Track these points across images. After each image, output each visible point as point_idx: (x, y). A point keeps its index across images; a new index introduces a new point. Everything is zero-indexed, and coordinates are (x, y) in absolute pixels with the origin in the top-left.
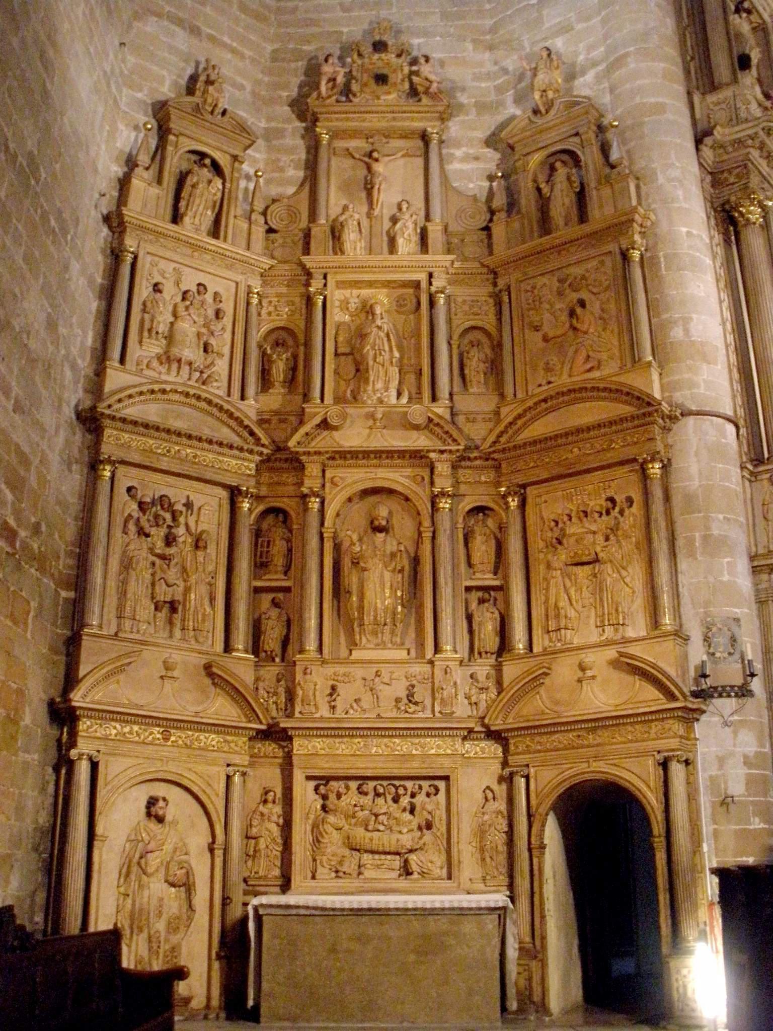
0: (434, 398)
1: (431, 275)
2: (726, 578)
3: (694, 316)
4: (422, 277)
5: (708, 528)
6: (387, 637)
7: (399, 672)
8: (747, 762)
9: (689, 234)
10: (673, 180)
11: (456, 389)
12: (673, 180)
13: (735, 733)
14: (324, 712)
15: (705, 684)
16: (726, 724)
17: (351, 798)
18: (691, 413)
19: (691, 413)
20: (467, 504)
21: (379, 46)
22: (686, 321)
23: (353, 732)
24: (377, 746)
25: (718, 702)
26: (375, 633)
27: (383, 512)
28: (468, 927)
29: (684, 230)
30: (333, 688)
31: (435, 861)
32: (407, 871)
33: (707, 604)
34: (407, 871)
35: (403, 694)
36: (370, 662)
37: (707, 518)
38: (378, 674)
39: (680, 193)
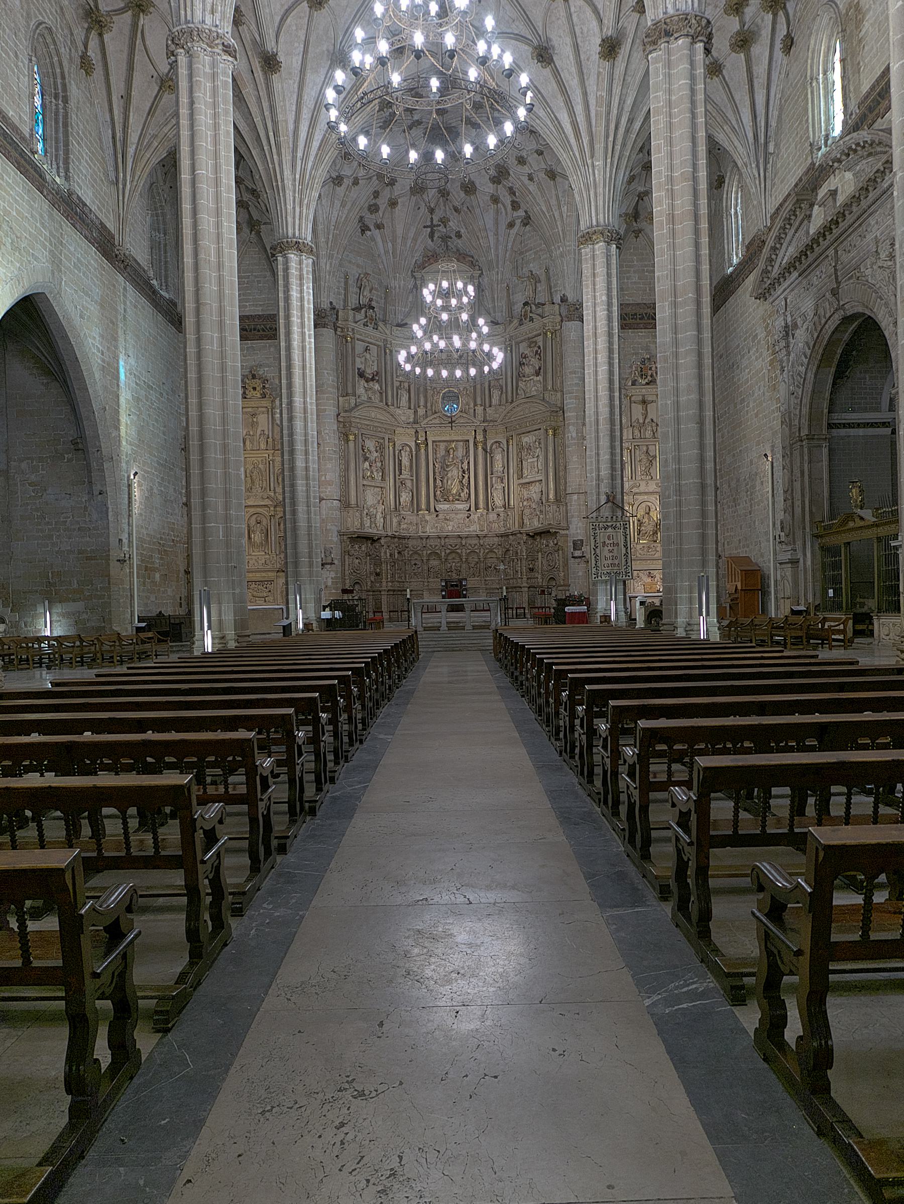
4: (267, 455)
7: (263, 557)
8: (332, 578)
17: (253, 586)
20: (279, 516)
21: (254, 377)
23: (252, 572)
24: (258, 575)
28: (276, 612)
31: (271, 598)
32: (265, 601)
34: (265, 601)
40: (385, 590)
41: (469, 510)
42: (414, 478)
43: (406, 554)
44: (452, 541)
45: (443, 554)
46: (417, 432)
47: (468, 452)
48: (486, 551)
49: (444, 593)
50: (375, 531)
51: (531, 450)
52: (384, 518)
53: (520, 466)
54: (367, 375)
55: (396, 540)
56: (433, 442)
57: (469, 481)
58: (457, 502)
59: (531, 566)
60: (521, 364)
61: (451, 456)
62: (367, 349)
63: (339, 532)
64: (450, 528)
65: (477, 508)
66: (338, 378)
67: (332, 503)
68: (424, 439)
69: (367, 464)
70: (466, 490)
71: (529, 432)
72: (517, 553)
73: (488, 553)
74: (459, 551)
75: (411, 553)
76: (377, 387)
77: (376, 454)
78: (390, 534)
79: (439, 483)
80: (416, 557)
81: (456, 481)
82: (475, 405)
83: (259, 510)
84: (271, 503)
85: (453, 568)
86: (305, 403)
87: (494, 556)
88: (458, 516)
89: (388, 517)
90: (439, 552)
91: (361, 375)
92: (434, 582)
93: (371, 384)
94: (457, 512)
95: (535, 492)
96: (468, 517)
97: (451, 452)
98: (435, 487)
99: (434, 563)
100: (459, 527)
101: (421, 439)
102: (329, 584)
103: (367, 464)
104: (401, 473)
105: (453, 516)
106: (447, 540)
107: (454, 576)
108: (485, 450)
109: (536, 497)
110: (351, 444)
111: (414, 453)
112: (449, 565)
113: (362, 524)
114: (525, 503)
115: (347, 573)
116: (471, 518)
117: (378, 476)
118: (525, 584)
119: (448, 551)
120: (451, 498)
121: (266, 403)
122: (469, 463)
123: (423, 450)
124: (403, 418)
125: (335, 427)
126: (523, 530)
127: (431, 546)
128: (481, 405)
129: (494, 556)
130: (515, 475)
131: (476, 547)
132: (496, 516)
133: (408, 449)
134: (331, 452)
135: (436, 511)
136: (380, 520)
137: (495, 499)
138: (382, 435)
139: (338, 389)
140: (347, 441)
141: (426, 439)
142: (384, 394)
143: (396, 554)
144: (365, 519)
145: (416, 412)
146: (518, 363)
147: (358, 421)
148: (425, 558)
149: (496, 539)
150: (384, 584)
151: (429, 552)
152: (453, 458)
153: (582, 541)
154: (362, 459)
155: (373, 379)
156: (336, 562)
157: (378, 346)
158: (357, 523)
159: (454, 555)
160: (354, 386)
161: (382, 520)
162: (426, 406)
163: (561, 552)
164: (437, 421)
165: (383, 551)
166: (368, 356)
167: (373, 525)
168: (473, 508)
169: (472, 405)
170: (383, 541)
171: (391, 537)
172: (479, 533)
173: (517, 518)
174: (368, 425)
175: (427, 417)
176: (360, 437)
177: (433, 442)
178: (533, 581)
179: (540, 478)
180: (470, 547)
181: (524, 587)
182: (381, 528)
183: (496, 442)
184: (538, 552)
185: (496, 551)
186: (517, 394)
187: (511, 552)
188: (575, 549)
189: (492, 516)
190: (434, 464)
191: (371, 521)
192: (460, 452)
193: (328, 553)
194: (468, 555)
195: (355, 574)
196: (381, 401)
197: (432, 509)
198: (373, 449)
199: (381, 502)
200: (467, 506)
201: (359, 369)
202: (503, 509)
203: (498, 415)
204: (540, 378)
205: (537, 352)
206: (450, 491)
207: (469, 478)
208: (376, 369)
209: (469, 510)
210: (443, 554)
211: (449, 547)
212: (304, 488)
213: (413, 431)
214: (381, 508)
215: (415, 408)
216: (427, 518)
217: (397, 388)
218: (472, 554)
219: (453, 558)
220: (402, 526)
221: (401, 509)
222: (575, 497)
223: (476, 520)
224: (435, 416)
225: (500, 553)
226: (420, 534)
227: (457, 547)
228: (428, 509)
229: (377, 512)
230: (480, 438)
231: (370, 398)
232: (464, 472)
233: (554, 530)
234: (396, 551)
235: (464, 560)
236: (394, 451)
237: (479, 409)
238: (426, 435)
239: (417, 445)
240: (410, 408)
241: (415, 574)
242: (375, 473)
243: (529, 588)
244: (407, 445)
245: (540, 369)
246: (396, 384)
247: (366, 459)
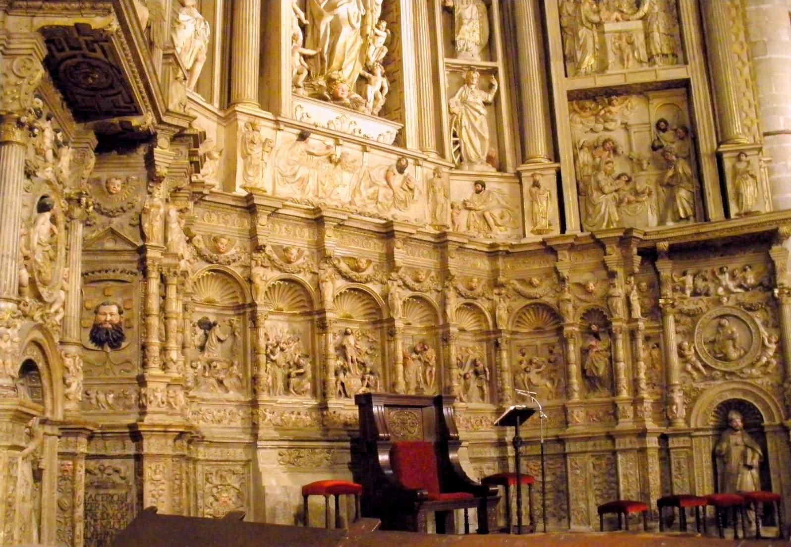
64: (343, 195)
70: (379, 81)
74: (375, 289)
85: (351, 352)
90: (305, 278)
96: (401, 170)
100: (375, 199)
179: (678, 73)
185: (484, 305)
202: (492, 171)
219: (348, 319)
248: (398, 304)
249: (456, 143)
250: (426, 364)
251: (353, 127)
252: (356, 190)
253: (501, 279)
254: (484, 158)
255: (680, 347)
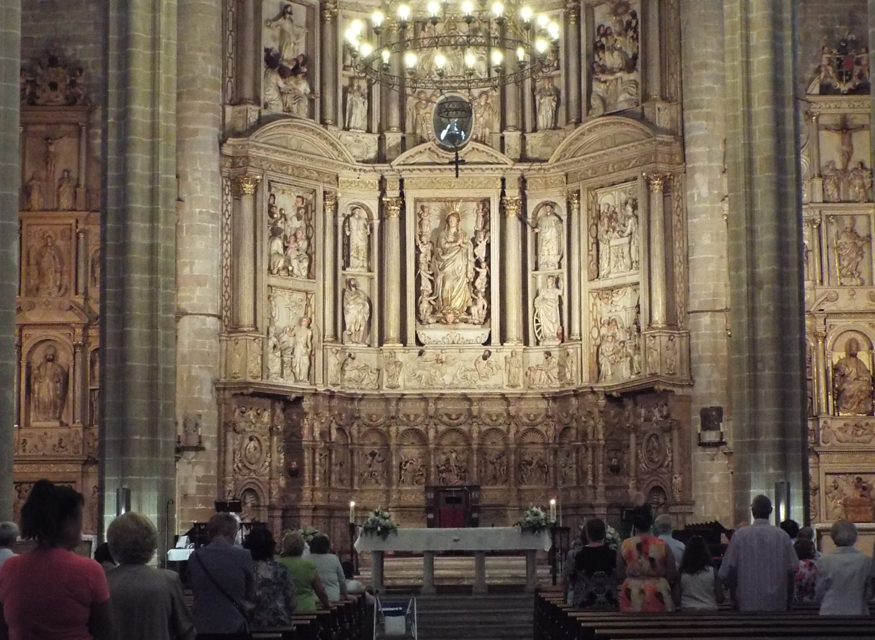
0: (77, 293)
1: (77, 222)
2: (196, 396)
3: (196, 261)
4: (73, 221)
5: (190, 372)
6: (51, 415)
8: (198, 480)
9: (201, 212)
10: (194, 180)
11: (89, 286)
12: (194, 180)
13: (193, 467)
14: (21, 453)
15: (635, 287)
16: (190, 463)
18: (187, 314)
19: (186, 314)
22: (192, 264)
23: (32, 462)
25: (186, 453)
26: (44, 413)
27: (51, 351)
29: (198, 210)
30: (25, 441)
33: (186, 407)
35: (56, 442)
36: (42, 428)
37: (190, 367)
38: (46, 434)
39: (199, 188)
40: (307, 507)
41: (488, 342)
42: (375, 274)
43: (355, 432)
44: (451, 407)
45: (432, 434)
46: (382, 182)
47: (487, 221)
48: (522, 429)
49: (431, 516)
50: (290, 382)
51: (616, 220)
52: (311, 356)
53: (594, 252)
54: (285, 64)
55: (335, 402)
56: (417, 201)
57: (489, 283)
58: (463, 325)
59: (614, 461)
60: (599, 48)
61: (453, 230)
62: (285, 12)
63: (216, 382)
64: (448, 379)
65: (503, 339)
66: (225, 67)
67: (204, 324)
68: (397, 193)
69: (277, 245)
70: (482, 302)
71: (613, 184)
72: (585, 435)
73: (525, 434)
74: (464, 428)
75: (364, 429)
76: (303, 87)
77: (295, 224)
78: (321, 389)
79: (426, 286)
80: (375, 438)
81: (463, 282)
82: (503, 127)
83: (52, 333)
84: (76, 319)
85: (453, 463)
86: (154, 115)
87: (538, 438)
88: (463, 355)
89: (319, 355)
90: (422, 428)
91: (273, 61)
92: (412, 492)
93: (292, 81)
94: (460, 346)
95: (625, 308)
97: (453, 220)
98: (418, 293)
99: (411, 452)
100: (465, 377)
101: (392, 193)
102: (192, 491)
103: (277, 245)
104: (347, 264)
105: (452, 353)
106: (440, 405)
107: (454, 480)
108: (522, 218)
109: (626, 318)
110: (247, 204)
111: (376, 223)
112: (443, 457)
113: (264, 367)
114: (604, 331)
115: (230, 468)
116: (491, 359)
117: (300, 267)
118: (601, 500)
119: (442, 428)
120: (450, 317)
121: (75, 116)
122: (488, 246)
123: (394, 218)
124: (356, 152)
125: (215, 167)
126: (599, 387)
127: (407, 416)
128: (516, 129)
129: (538, 438)
130: (584, 273)
131: (501, 420)
132: (542, 356)
133: (364, 214)
134: (205, 217)
135: (418, 343)
136: (301, 360)
137: (541, 320)
138: (311, 184)
139: (224, 89)
140: (238, 193)
141: (402, 195)
142: (318, 102)
143: (334, 433)
144: (271, 356)
145: (381, 140)
146: (591, 47)
147: (262, 153)
148: (393, 442)
149: (543, 404)
150: (307, 494)
151: (402, 429)
152: (456, 235)
153: (719, 410)
154: (267, 233)
155: (295, 72)
156: (207, 445)
157: (310, 7)
158: (254, 366)
159: (454, 436)
160: (256, 85)
161: (306, 360)
162: (402, 128)
163: (675, 433)
164: (425, 158)
165: (306, 423)
166: (287, 25)
167: (287, 371)
168: (496, 339)
169: (497, 126)
170: (306, 404)
171: (324, 395)
172: (507, 390)
173: (586, 362)
174: (283, 165)
175: (404, 150)
176: (266, 188)
177: (417, 201)
178: (618, 493)
180: (488, 420)
181: (599, 506)
182: (303, 376)
183: (546, 204)
184: (629, 434)
186: (589, 107)
187: (573, 431)
188: (706, 427)
189: (536, 356)
190: (417, 247)
191: (283, 362)
192: (472, 223)
193: (191, 426)
194: (483, 436)
195: (245, 471)
196: (311, 116)
197: (411, 339)
198: (290, 212)
199: (305, 322)
200: (482, 334)
201: (268, 51)
202: (558, 342)
203: (549, 150)
204: (634, 76)
205: (629, 23)
206: (447, 302)
207: (488, 276)
208: (302, 50)
209: (488, 342)
210: (432, 434)
211: (445, 419)
212: (146, 290)
213: (374, 178)
214: (304, 334)
215: (381, 131)
216: (401, 357)
217: (345, 91)
218: (493, 435)
219: (454, 444)
220: (348, 374)
221: (346, 338)
222: (706, 319)
223: (502, 362)
224: (421, 147)
225: (551, 433)
226: (385, 390)
227: (462, 418)
228: (403, 340)
229: (295, 343)
230: (513, 193)
231: (289, 110)
232: (478, 263)
233: (662, 388)
234: (334, 426)
235: (475, 447)
236: (335, 216)
237: (512, 137)
238: (402, 187)
239: (382, 206)
240: (369, 131)
241: (371, 474)
242: (295, 263)
243: (609, 507)
244: (362, 206)
245: (635, 57)
246: (343, 82)
247: (275, 233)
248: (475, 435)
249: (538, 327)
250: (501, 466)
251: (457, 338)
252: (455, 376)
253: (550, 413)
254: (555, 335)
255: (637, 455)
